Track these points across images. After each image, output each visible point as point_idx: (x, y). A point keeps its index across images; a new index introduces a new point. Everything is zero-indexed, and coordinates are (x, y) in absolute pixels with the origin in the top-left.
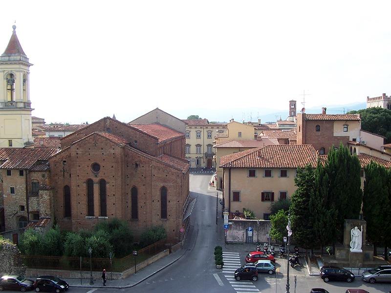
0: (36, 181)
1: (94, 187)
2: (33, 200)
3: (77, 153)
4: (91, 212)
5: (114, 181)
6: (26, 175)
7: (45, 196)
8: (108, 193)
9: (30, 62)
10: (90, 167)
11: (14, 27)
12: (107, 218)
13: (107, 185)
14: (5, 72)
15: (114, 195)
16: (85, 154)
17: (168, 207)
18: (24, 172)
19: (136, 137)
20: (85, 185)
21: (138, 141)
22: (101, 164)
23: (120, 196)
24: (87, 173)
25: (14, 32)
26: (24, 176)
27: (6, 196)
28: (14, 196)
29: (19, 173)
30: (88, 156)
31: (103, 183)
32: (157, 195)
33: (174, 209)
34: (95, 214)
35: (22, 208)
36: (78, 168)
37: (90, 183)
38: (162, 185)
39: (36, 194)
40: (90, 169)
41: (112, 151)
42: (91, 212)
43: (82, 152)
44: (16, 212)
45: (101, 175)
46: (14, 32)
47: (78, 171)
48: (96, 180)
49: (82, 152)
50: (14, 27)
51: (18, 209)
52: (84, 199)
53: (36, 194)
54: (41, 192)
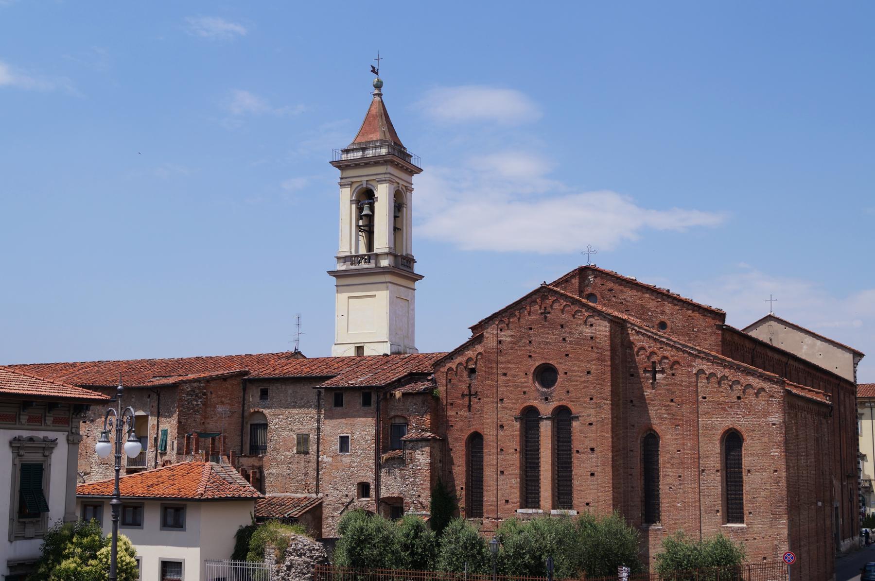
0: (402, 421)
1: (542, 430)
3: (500, 342)
4: (530, 498)
5: (592, 412)
6: (378, 403)
8: (576, 445)
9: (414, 162)
10: (531, 377)
12: (573, 512)
13: (575, 424)
14: (355, 186)
15: (592, 450)
16: (521, 340)
17: (746, 488)
18: (374, 398)
19: (663, 312)
20: (517, 425)
21: (669, 323)
22: (561, 368)
23: (610, 453)
24: (524, 393)
26: (373, 405)
27: (330, 459)
28: (346, 459)
29: (361, 401)
30: (528, 347)
33: (763, 494)
34: (542, 503)
35: (364, 490)
36: (501, 379)
41: (588, 331)
42: (530, 498)
43: (512, 336)
44: (348, 500)
45: (559, 396)
47: (501, 389)
48: (546, 409)
49: (512, 336)
51: (354, 492)
52: (513, 460)
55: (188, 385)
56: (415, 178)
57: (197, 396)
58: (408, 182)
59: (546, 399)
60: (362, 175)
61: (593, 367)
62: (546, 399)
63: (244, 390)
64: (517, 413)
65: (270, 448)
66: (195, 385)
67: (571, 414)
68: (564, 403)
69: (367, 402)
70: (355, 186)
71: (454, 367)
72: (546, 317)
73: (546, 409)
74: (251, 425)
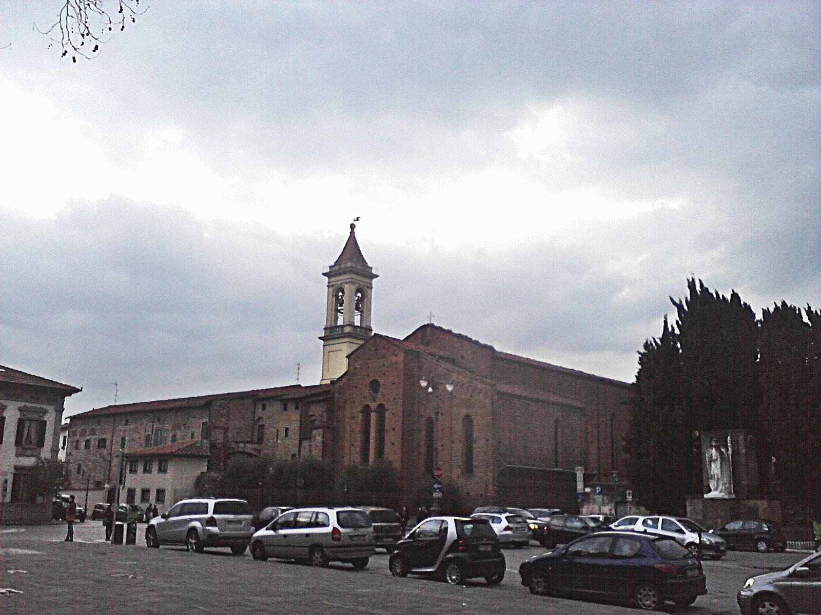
2: (306, 444)
3: (355, 368)
7: (318, 437)
11: (352, 226)
13: (387, 413)
22: (381, 381)
25: (352, 233)
31: (381, 409)
32: (459, 429)
36: (354, 389)
37: (366, 410)
38: (465, 411)
39: (309, 438)
40: (367, 391)
46: (352, 233)
48: (373, 406)
50: (352, 226)
53: (309, 438)
54: (314, 432)
55: (218, 401)
56: (374, 281)
57: (223, 408)
58: (369, 284)
59: (374, 400)
60: (338, 280)
61: (396, 381)
62: (374, 400)
63: (255, 405)
64: (360, 408)
65: (265, 439)
66: (222, 401)
67: (385, 408)
68: (382, 402)
69: (297, 408)
70: (335, 287)
71: (342, 385)
72: (376, 353)
73: (373, 406)
74: (259, 426)
